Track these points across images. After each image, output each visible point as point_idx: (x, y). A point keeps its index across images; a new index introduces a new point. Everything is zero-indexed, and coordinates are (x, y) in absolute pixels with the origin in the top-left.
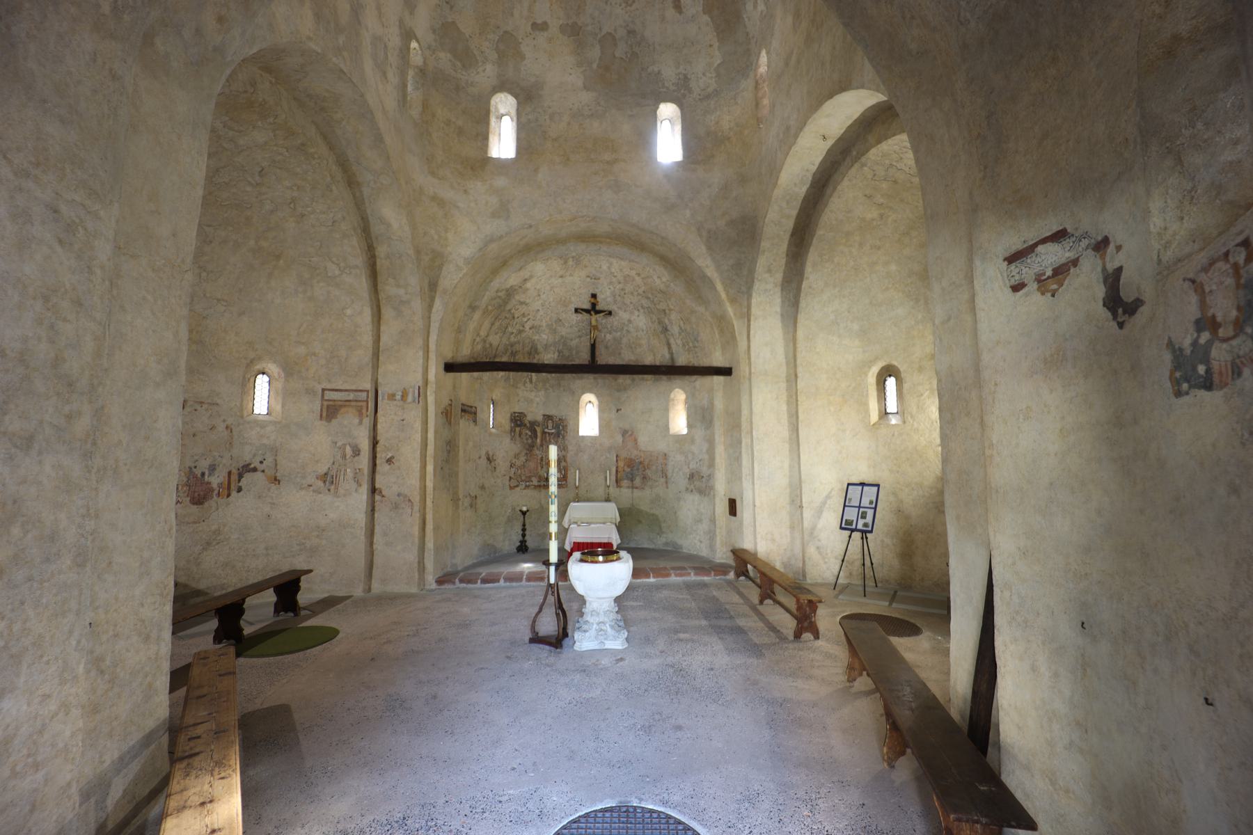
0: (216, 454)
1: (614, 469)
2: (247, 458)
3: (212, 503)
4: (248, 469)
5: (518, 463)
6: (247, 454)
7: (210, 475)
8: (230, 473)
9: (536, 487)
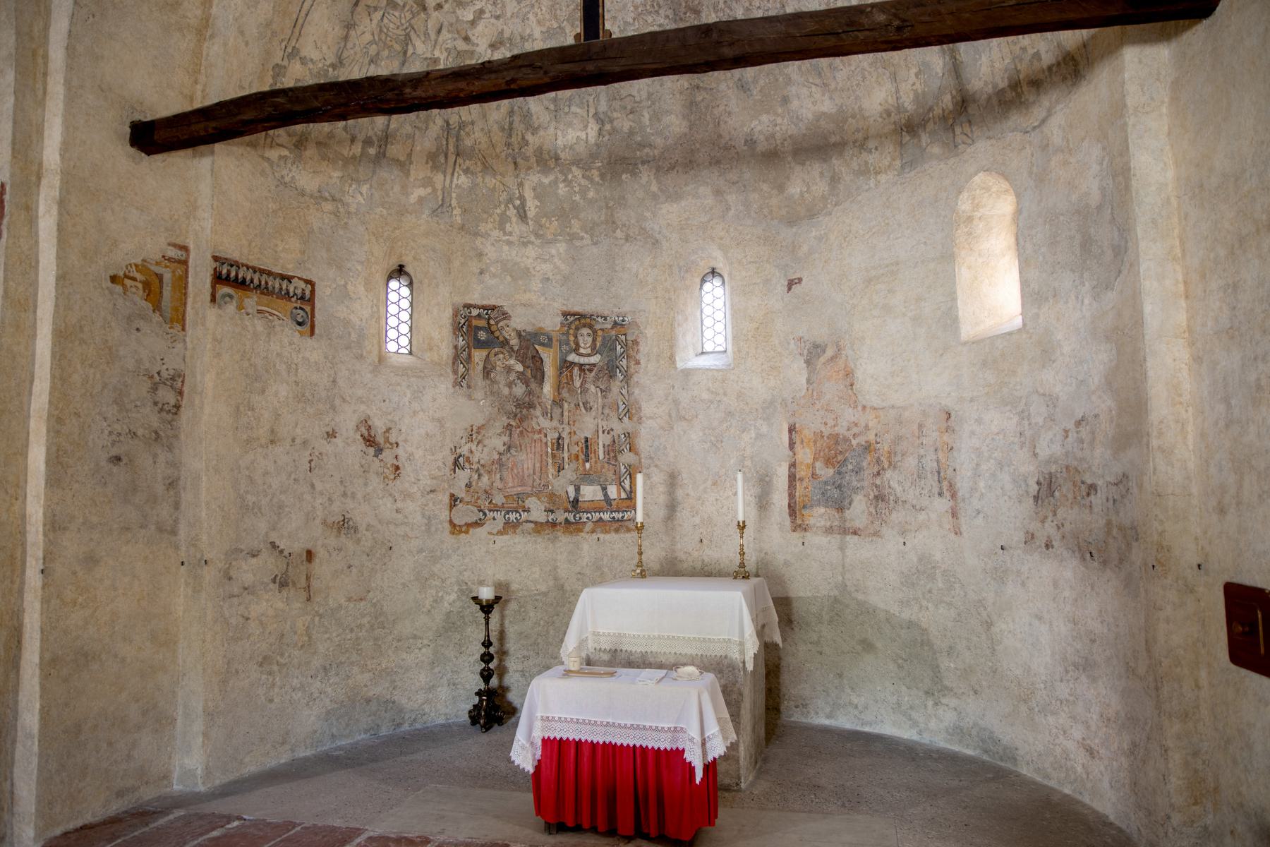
1: (782, 473)
5: (481, 455)
9: (539, 527)
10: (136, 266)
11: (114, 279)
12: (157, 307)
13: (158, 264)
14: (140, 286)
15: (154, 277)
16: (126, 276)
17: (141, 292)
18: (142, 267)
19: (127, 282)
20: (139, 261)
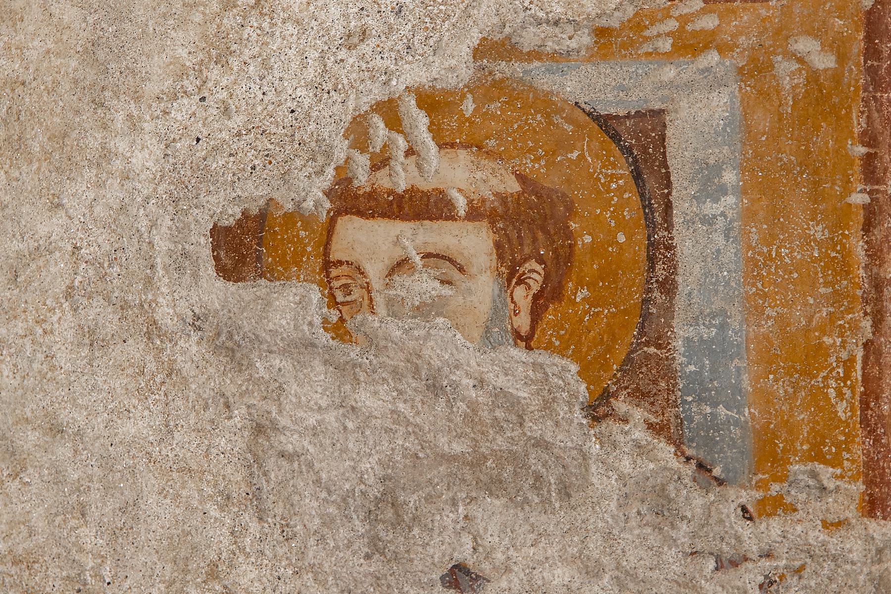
10: (432, 102)
11: (245, 247)
12: (630, 370)
13: (607, 40)
14: (475, 243)
15: (589, 153)
16: (349, 200)
17: (483, 287)
18: (491, 101)
19: (368, 241)
20: (453, 66)
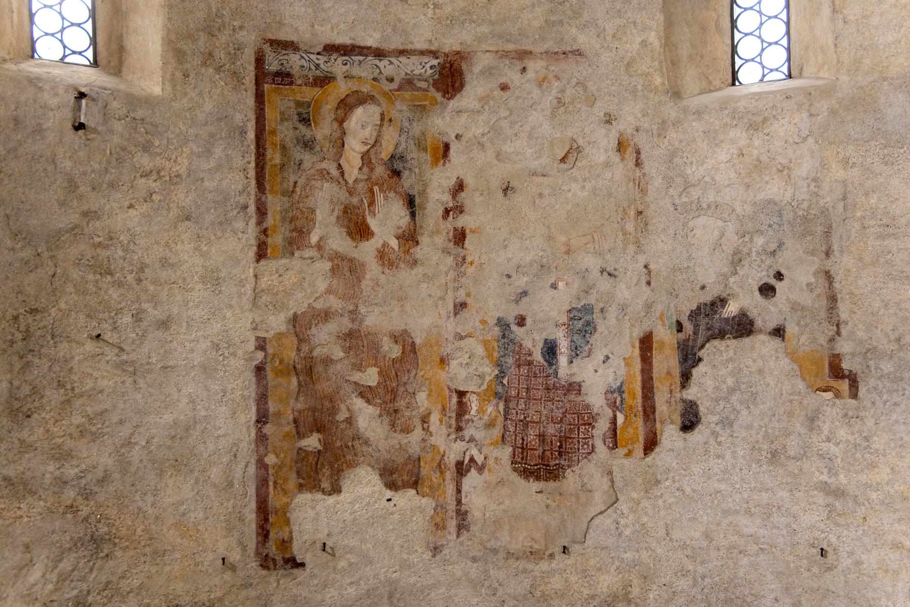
0: (592, 263)
2: (709, 274)
3: (589, 473)
4: (714, 323)
6: (702, 257)
7: (575, 352)
8: (646, 343)
